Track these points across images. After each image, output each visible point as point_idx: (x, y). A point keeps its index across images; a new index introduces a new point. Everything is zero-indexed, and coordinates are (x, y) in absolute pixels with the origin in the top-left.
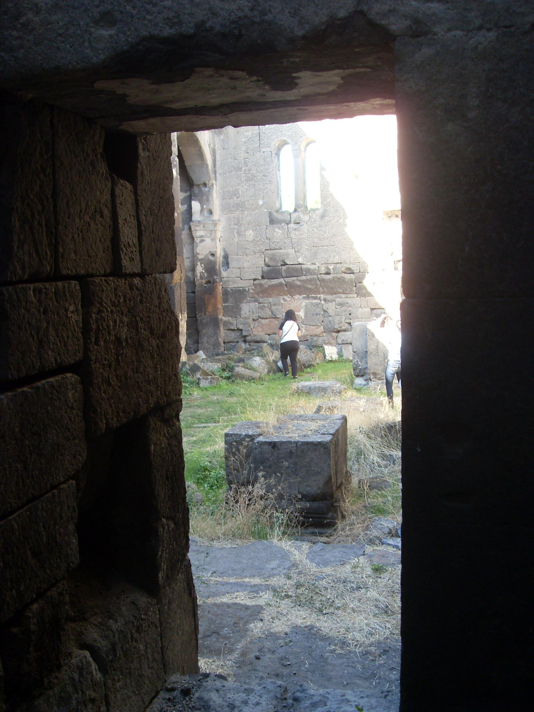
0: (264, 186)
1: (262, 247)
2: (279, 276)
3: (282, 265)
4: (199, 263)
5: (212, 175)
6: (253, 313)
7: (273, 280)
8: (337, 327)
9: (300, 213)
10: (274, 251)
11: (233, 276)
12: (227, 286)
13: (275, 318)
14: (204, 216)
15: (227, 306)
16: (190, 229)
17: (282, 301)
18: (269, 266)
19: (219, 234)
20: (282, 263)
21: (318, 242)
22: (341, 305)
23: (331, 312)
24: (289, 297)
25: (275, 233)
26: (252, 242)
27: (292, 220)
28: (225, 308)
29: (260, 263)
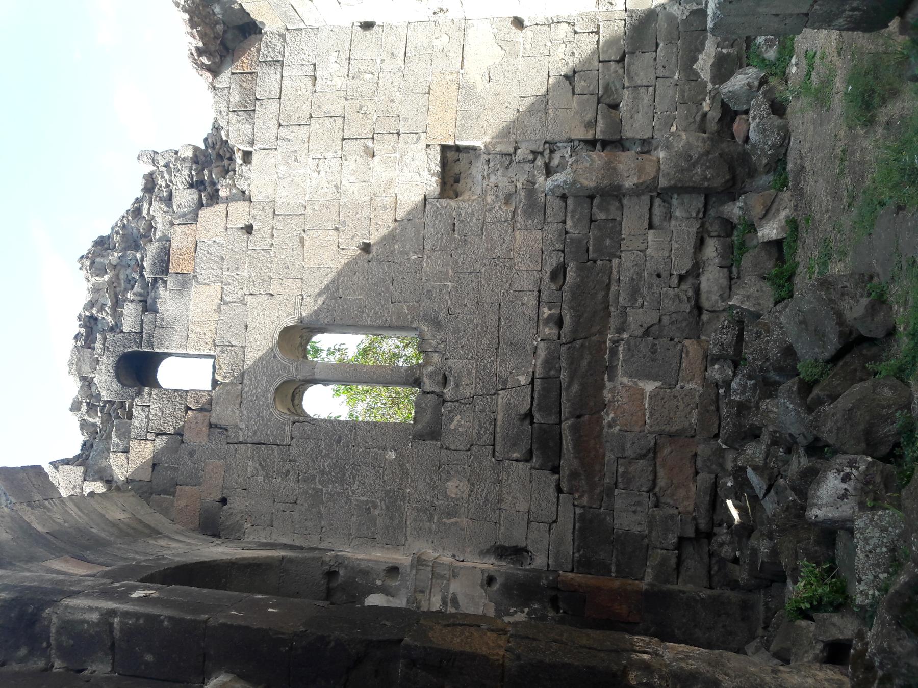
0: (358, 445)
1: (487, 463)
2: (556, 430)
3: (532, 423)
4: (507, 619)
6: (638, 504)
7: (564, 446)
9: (425, 372)
10: (498, 435)
11: (546, 542)
12: (570, 560)
13: (655, 453)
15: (617, 566)
18: (531, 452)
19: (447, 559)
20: (528, 422)
21: (488, 337)
22: (634, 293)
24: (608, 415)
25: (460, 430)
26: (473, 484)
27: (436, 389)
28: (621, 574)
29: (521, 472)
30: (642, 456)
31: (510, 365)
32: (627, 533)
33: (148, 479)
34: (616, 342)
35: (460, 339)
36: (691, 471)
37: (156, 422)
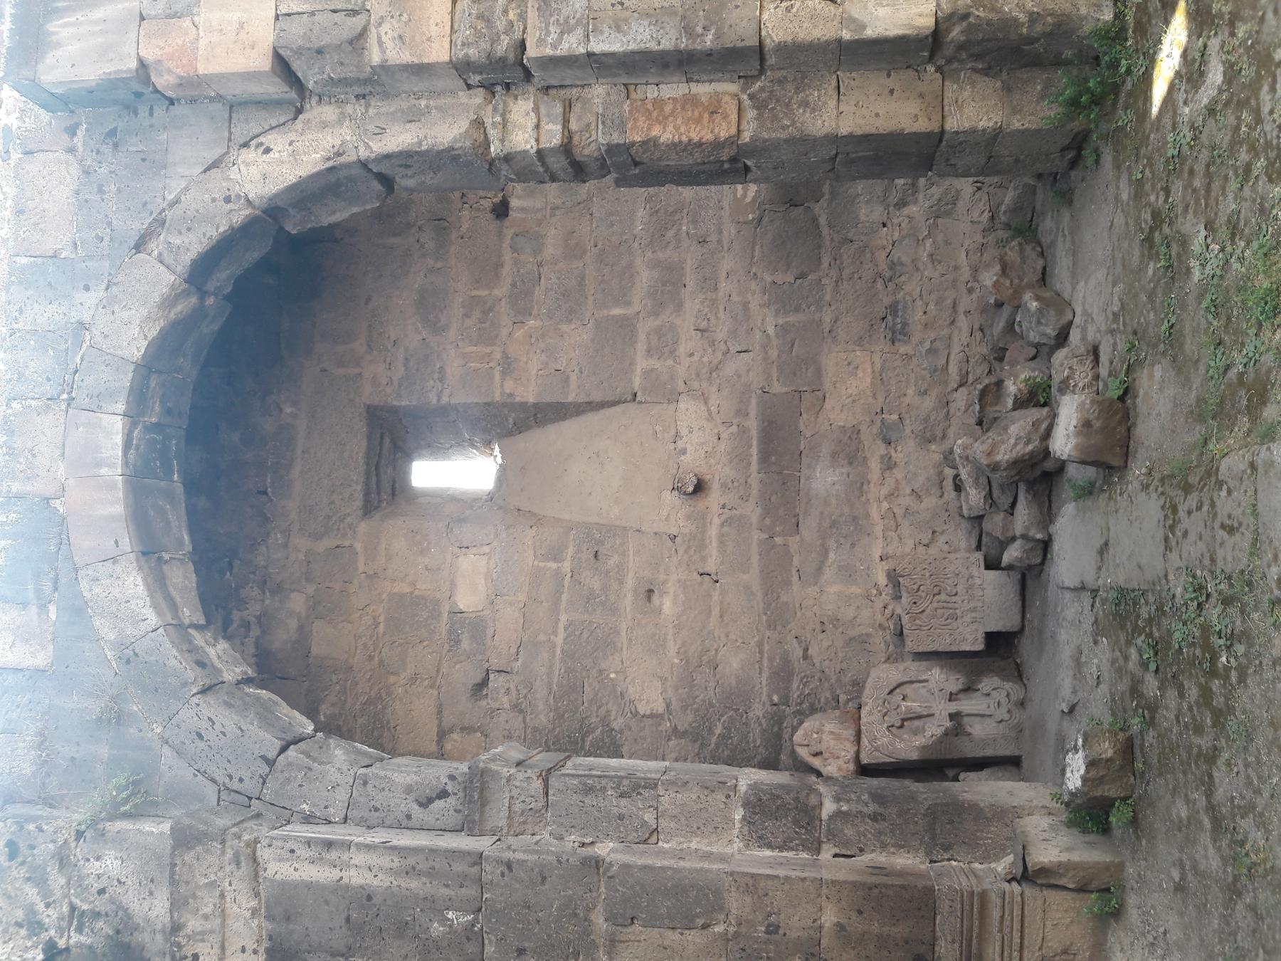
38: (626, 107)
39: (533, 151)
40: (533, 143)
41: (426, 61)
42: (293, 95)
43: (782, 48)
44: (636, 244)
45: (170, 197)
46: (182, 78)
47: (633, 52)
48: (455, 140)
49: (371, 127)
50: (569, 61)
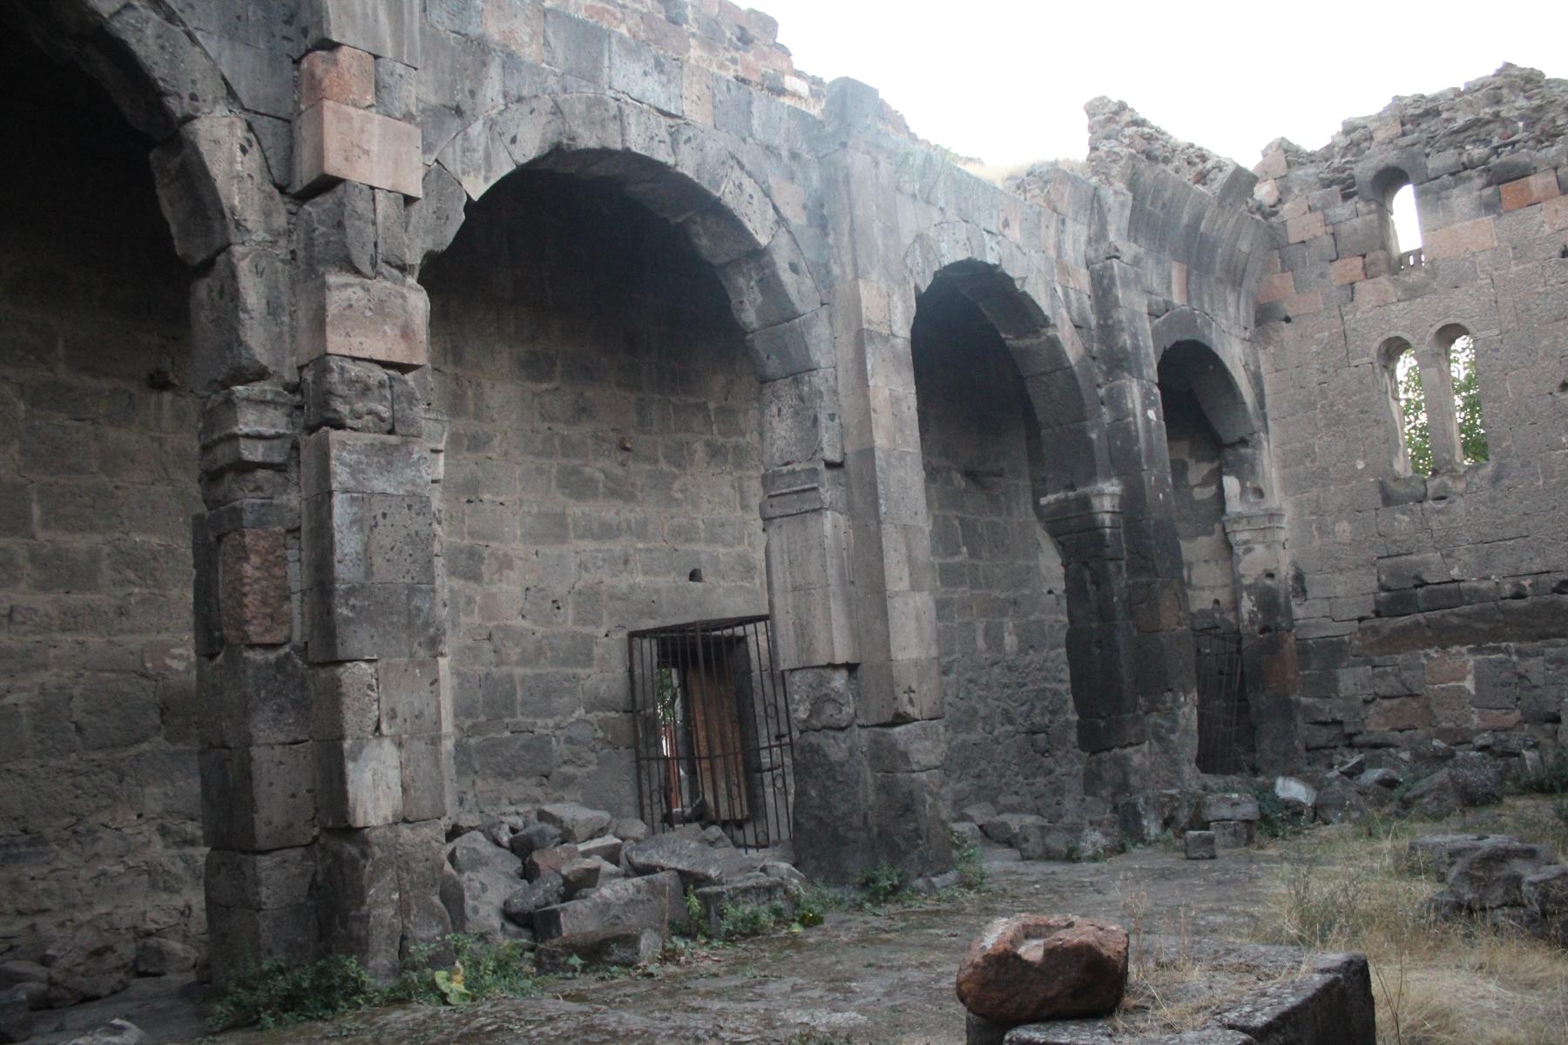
1: (1371, 553)
5: (1257, 424)
8: (1552, 709)
14: (1247, 502)
16: (1224, 529)
17: (1425, 661)
23: (1536, 678)
27: (1430, 493)
30: (1403, 684)
31: (1467, 558)
32: (1336, 680)
33: (1291, 241)
34: (1507, 651)
35: (1484, 504)
36: (1400, 725)
37: (1345, 229)
38: (278, 529)
39: (236, 430)
40: (246, 430)
41: (328, 329)
42: (297, 187)
43: (336, 683)
44: (117, 535)
45: (198, 35)
46: (320, 82)
47: (332, 536)
48: (248, 348)
49: (263, 263)
50: (325, 473)
